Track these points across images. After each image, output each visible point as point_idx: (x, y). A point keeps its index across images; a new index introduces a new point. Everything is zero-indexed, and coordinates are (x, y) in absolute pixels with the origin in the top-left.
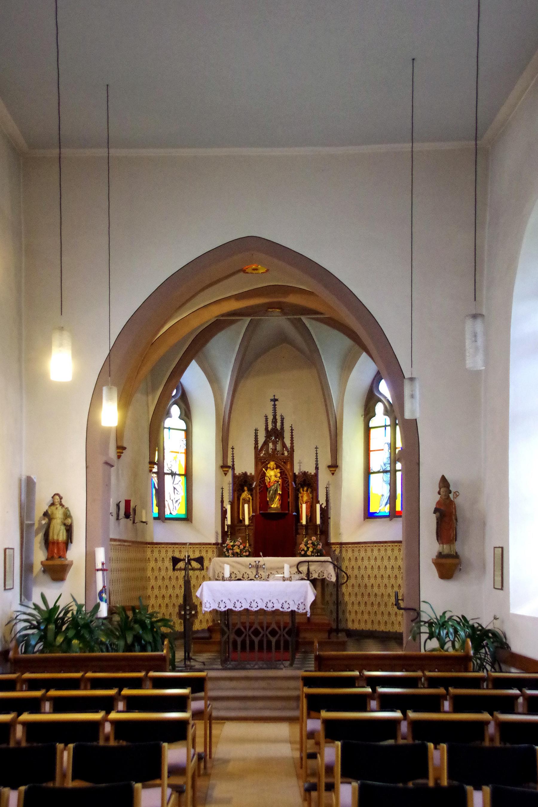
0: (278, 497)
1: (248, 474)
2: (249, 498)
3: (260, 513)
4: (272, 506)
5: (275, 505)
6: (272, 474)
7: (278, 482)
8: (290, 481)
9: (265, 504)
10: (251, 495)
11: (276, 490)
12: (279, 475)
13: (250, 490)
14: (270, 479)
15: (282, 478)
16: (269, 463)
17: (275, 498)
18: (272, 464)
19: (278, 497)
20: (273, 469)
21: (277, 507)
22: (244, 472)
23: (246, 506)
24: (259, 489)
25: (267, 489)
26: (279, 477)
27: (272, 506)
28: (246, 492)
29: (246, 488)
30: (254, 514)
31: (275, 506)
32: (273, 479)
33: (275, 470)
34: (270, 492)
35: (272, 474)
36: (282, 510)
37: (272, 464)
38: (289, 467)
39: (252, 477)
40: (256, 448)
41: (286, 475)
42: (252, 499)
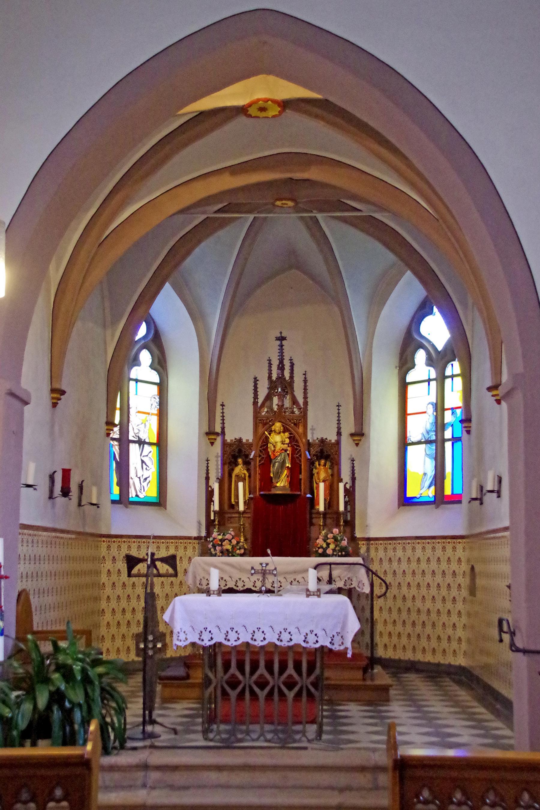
3: (261, 495)
4: (278, 485)
5: (282, 484)
6: (278, 440)
7: (286, 451)
9: (267, 482)
11: (284, 462)
12: (287, 441)
14: (274, 447)
15: (292, 446)
16: (273, 424)
17: (282, 473)
20: (280, 433)
21: (284, 486)
23: (241, 485)
24: (260, 461)
25: (271, 460)
26: (288, 444)
27: (278, 485)
30: (252, 496)
31: (282, 485)
32: (279, 446)
33: (282, 434)
34: (274, 466)
35: (278, 440)
36: (291, 490)
38: (301, 430)
41: (297, 441)
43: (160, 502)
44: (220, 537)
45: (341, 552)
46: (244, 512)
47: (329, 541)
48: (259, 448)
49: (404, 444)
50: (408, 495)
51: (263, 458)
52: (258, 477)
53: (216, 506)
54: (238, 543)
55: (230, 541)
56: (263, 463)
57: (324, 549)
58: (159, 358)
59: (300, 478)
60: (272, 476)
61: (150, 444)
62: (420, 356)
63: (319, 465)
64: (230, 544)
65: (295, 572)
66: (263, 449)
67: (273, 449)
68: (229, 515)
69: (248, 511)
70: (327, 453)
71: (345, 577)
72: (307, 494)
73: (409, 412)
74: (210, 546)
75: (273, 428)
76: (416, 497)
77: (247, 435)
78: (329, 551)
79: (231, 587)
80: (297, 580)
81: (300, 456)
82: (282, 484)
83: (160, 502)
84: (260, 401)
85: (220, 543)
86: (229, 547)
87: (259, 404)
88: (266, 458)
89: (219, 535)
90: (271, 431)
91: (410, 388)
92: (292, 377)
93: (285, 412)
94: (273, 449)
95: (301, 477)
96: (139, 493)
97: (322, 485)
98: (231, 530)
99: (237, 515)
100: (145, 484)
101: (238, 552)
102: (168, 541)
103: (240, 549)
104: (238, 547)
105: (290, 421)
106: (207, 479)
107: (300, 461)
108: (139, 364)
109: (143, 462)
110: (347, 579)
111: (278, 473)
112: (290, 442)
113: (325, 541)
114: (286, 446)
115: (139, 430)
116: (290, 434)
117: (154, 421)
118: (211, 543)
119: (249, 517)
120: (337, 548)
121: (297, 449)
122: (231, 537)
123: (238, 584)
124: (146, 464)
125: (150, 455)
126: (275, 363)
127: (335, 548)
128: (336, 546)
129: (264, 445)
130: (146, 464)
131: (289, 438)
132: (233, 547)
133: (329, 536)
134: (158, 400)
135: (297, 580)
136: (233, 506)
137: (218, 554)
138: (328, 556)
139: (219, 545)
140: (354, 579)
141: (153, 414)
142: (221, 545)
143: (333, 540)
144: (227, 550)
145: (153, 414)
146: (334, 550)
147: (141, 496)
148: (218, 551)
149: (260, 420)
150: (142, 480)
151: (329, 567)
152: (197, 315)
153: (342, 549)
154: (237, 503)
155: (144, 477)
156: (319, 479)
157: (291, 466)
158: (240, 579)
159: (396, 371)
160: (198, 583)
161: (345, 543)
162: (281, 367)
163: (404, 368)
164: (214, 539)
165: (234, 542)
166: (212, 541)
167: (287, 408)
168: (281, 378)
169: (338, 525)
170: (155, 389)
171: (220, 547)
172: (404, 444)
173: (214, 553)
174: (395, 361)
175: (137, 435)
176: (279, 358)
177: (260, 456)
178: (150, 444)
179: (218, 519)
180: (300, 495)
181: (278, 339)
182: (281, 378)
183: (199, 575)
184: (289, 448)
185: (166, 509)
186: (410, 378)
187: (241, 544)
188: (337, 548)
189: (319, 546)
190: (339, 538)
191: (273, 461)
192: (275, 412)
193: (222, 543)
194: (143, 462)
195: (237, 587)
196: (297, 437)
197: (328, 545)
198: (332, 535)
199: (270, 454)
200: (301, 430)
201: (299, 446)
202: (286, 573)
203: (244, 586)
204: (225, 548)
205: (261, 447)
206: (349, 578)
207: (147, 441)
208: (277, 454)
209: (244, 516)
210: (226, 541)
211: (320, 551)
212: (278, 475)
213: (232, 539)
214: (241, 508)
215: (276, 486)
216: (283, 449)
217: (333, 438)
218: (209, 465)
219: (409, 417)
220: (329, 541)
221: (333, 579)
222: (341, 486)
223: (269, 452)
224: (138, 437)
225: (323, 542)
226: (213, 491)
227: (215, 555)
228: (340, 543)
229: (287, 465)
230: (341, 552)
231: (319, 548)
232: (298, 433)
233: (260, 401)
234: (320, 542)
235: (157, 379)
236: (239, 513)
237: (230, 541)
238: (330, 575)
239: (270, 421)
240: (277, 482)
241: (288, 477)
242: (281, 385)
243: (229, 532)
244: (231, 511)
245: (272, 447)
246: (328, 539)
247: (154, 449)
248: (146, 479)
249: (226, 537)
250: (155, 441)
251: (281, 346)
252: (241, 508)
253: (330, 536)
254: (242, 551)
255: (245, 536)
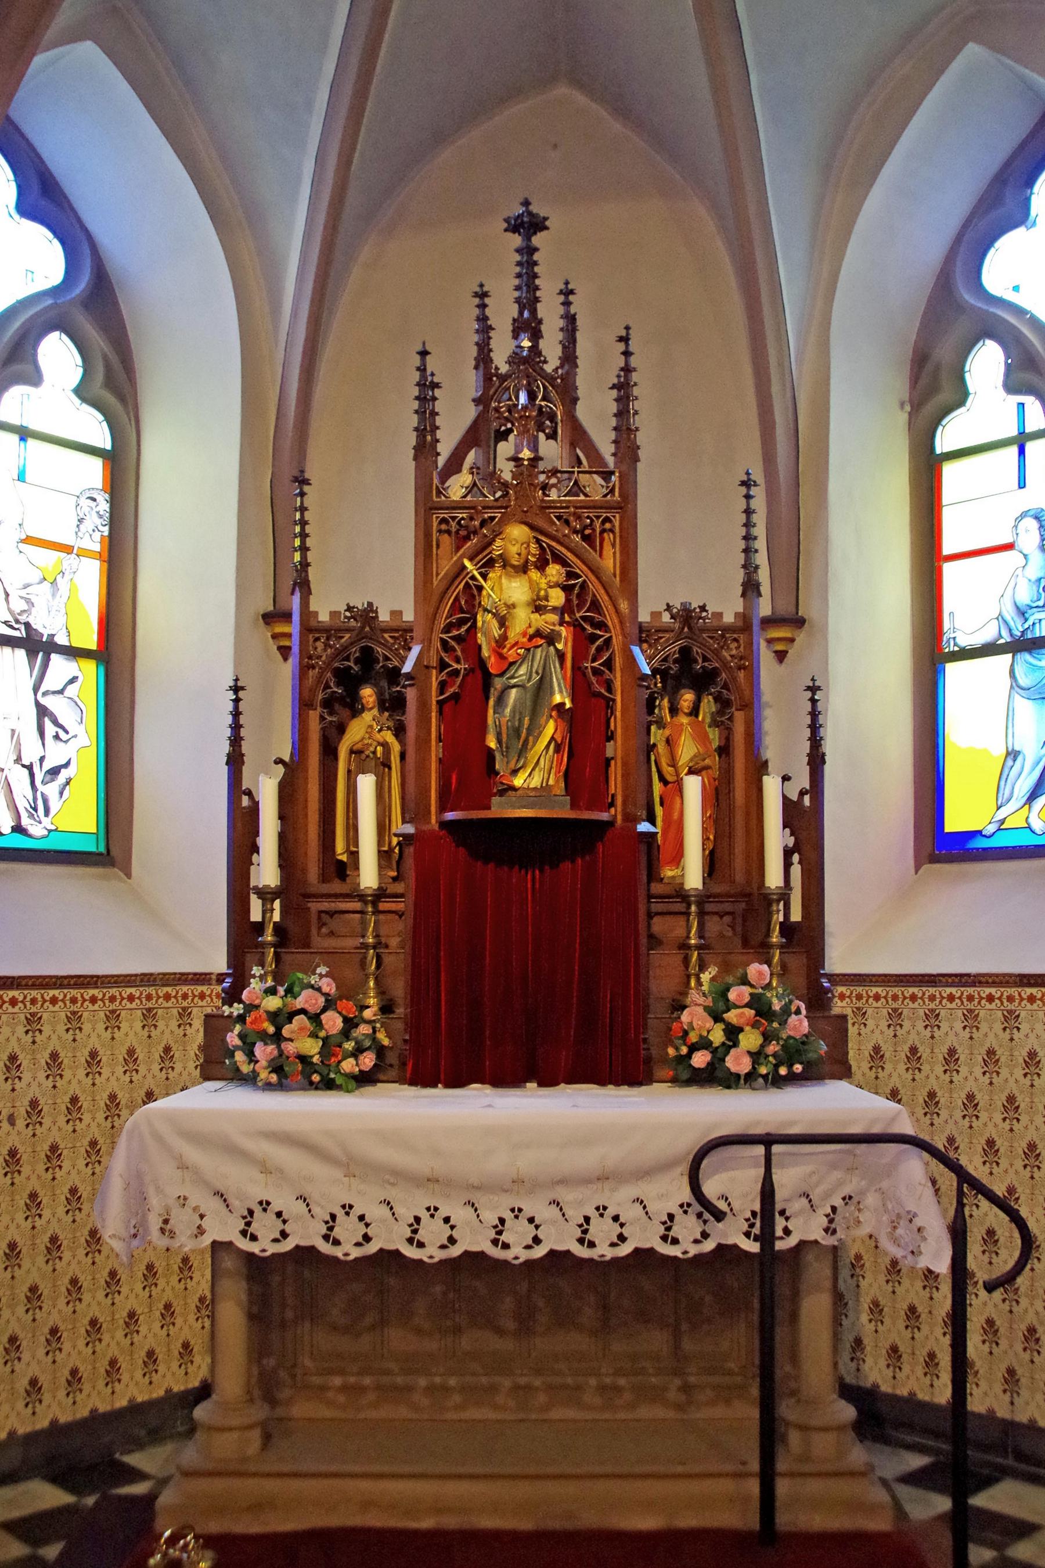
0: (550, 729)
1: (384, 617)
2: (385, 745)
3: (444, 825)
4: (518, 781)
7: (551, 639)
8: (617, 642)
10: (399, 731)
11: (542, 687)
12: (557, 598)
13: (393, 704)
14: (502, 622)
15: (576, 625)
16: (497, 534)
17: (535, 731)
18: (516, 538)
19: (550, 729)
20: (523, 569)
21: (545, 789)
22: (360, 603)
23: (366, 784)
24: (442, 686)
25: (487, 679)
26: (561, 611)
27: (518, 781)
28: (367, 717)
29: (367, 693)
30: (409, 829)
31: (536, 782)
32: (523, 620)
33: (534, 574)
34: (501, 701)
36: (574, 806)
37: (516, 538)
39: (404, 634)
40: (425, 447)
41: (595, 606)
42: (403, 756)
43: (110, 853)
44: (273, 1003)
45: (790, 1066)
46: (380, 894)
47: (732, 1016)
48: (437, 635)
49: (933, 654)
50: (953, 824)
51: (456, 672)
52: (435, 751)
53: (267, 871)
54: (351, 1025)
55: (315, 1019)
56: (455, 697)
57: (714, 1051)
58: (105, 358)
59: (609, 753)
60: (493, 745)
61: (73, 653)
62: (987, 364)
63: (674, 710)
64: (314, 1035)
65: (603, 1177)
66: (458, 639)
67: (496, 632)
68: (326, 905)
69: (399, 888)
70: (705, 666)
71: (828, 1195)
72: (637, 820)
73: (947, 550)
74: (233, 1039)
75: (497, 548)
76: (979, 832)
77: (396, 598)
78: (738, 1062)
79: (304, 1243)
80: (611, 1212)
81: (609, 664)
82: (534, 778)
83: (110, 853)
84: (445, 450)
85: (271, 1030)
86: (311, 1047)
87: (441, 461)
88: (469, 672)
89: (272, 991)
90: (490, 563)
91: (949, 470)
92: (569, 357)
93: (545, 487)
94: (496, 632)
95: (610, 750)
96: (25, 821)
97: (693, 787)
98: (322, 970)
99: (357, 906)
100: (51, 790)
101: (349, 1065)
102: (114, 991)
103: (357, 1052)
104: (349, 1046)
105: (567, 522)
106: (235, 761)
107: (609, 686)
108: (34, 378)
109: (42, 712)
110: (838, 1202)
111: (517, 731)
112: (566, 609)
113: (717, 1018)
114: (554, 618)
115: (28, 601)
116: (571, 575)
117: (88, 580)
118: (238, 1028)
119: (401, 915)
120: (773, 1048)
121: (594, 638)
122: (321, 1001)
123: (337, 1232)
124: (56, 722)
125: (72, 691)
126: (503, 311)
127: (762, 1046)
128: (767, 1037)
129: (461, 622)
130: (56, 722)
131: (567, 589)
132: (328, 1046)
133: (732, 995)
134: (104, 506)
135: (611, 1212)
136: (343, 870)
137: (263, 1075)
138: (731, 1081)
139: (264, 1037)
140: (871, 1200)
141: (83, 553)
142: (278, 1038)
143: (750, 1013)
144: (303, 1059)
145: (83, 553)
146: (756, 1056)
147: (36, 830)
148: (263, 1063)
149: (444, 521)
150: (39, 777)
151: (760, 1150)
152: (234, 214)
153: (793, 1051)
154: (354, 855)
155: (48, 765)
156: (673, 764)
157: (573, 701)
158: (348, 1208)
159: (902, 418)
160: (154, 1223)
161: (799, 1024)
162: (528, 325)
163: (930, 408)
164: (251, 1008)
165: (333, 1022)
166: (241, 1019)
167: (555, 472)
168: (528, 363)
169: (762, 951)
170: (93, 471)
171: (271, 1048)
172: (933, 654)
173: (246, 1069)
174: (896, 385)
175: (23, 618)
176: (517, 294)
177: (443, 665)
178: (73, 653)
179: (283, 922)
180: (611, 824)
181: (515, 226)
182: (528, 363)
183: (159, 1190)
184: (563, 631)
185: (129, 875)
186: (946, 439)
187: (364, 1029)
188: (773, 1048)
189: (693, 1037)
190: (777, 1005)
191: (498, 683)
192: (505, 485)
193: (279, 1029)
194: (42, 712)
195: (337, 1242)
196: (594, 587)
197: (733, 1033)
198: (746, 990)
199: (485, 653)
200: (609, 561)
201: (602, 626)
202: (563, 1182)
203: (367, 1238)
204: (290, 1048)
205: (447, 629)
206: (847, 1199)
207: (61, 640)
208: (511, 655)
209: (383, 906)
210: (300, 1020)
211: (700, 1059)
212: (519, 740)
213: (324, 1010)
214: (369, 877)
215: (514, 789)
216: (538, 634)
217: (728, 607)
218: (242, 706)
219: (948, 568)
220: (732, 1016)
221: (778, 1207)
222: (772, 788)
223: (480, 647)
224: (27, 625)
225: (709, 1023)
226: (254, 810)
227: (249, 1080)
228: (783, 1023)
229: (558, 699)
230: (790, 1066)
231: (693, 1048)
232: (595, 572)
233: (445, 450)
234: (695, 1017)
235: (102, 438)
236: (361, 897)
237: (315, 1019)
238: (767, 1192)
239: (483, 524)
240: (515, 772)
241: (558, 749)
242: (527, 392)
243: (313, 980)
244: (337, 887)
245: (495, 624)
246: (729, 1006)
247: (89, 672)
248: (54, 772)
249: (299, 1003)
250: (91, 643)
251: (528, 251)
252: (369, 877)
253: (738, 993)
254: (368, 1060)
255: (381, 992)
